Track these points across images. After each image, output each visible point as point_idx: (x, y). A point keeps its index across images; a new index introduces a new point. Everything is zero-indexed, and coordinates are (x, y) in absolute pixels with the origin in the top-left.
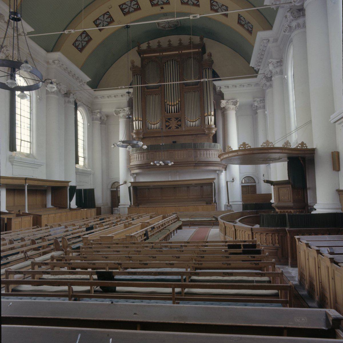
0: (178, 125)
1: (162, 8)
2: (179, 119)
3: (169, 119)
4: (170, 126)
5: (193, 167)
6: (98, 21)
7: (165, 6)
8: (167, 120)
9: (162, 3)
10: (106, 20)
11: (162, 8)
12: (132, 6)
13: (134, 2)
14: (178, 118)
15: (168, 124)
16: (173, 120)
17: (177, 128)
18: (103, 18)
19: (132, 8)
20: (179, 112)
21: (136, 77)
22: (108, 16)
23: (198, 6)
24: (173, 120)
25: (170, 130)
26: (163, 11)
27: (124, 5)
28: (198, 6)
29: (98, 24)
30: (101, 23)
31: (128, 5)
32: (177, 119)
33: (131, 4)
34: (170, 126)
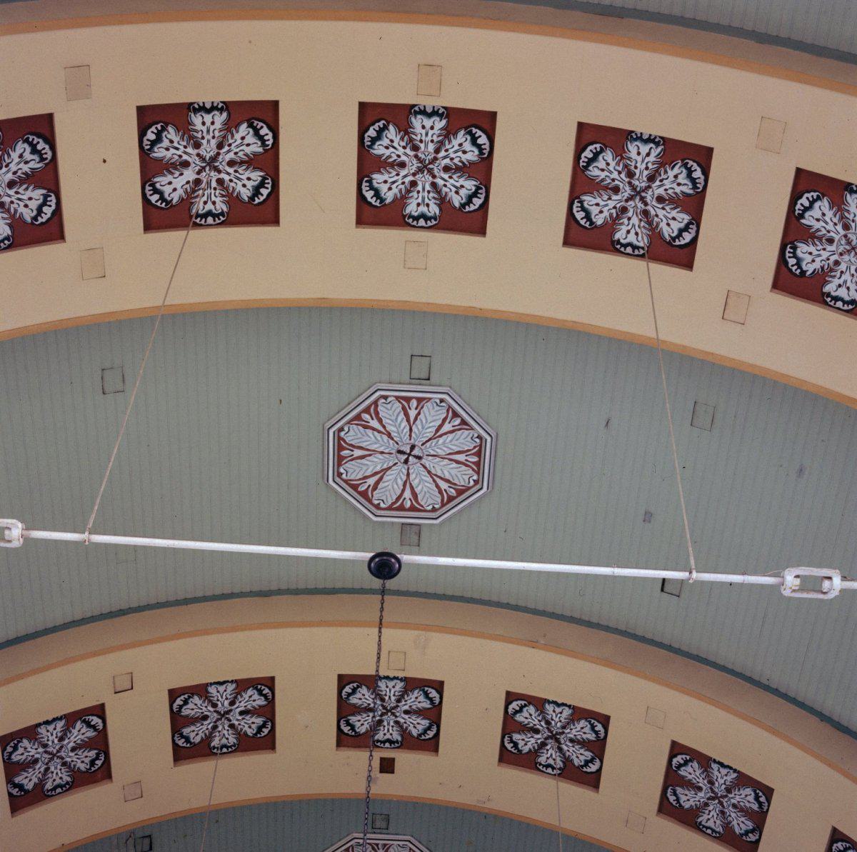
1: (387, 766)
6: (25, 742)
7: (403, 758)
9: (396, 736)
10: (71, 757)
11: (387, 766)
12: (235, 717)
13: (256, 696)
18: (61, 739)
19: (232, 726)
22: (91, 733)
23: (593, 781)
26: (385, 786)
27: (196, 699)
28: (593, 781)
29: (18, 762)
30: (36, 761)
31: (215, 705)
33: (232, 703)
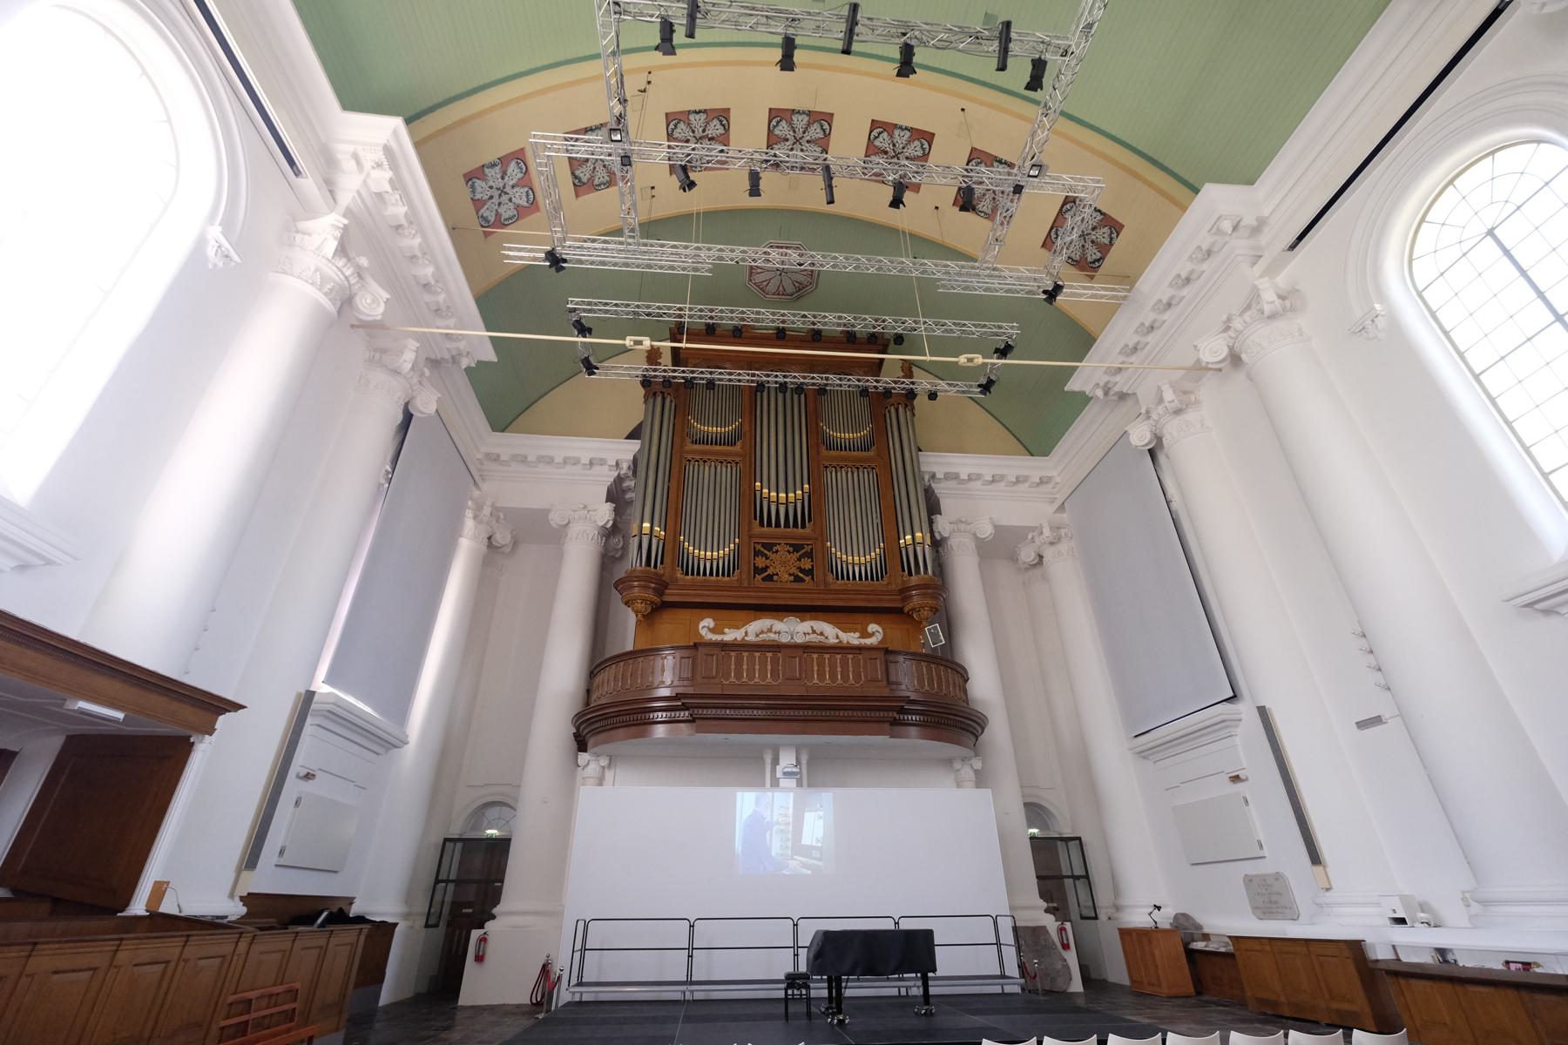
0: (802, 571)
2: (808, 549)
3: (769, 547)
4: (769, 572)
5: (887, 726)
8: (759, 547)
14: (802, 547)
15: (761, 562)
16: (782, 549)
17: (797, 579)
20: (803, 526)
21: (659, 399)
24: (782, 549)
25: (769, 584)
32: (797, 548)
34: (769, 572)
